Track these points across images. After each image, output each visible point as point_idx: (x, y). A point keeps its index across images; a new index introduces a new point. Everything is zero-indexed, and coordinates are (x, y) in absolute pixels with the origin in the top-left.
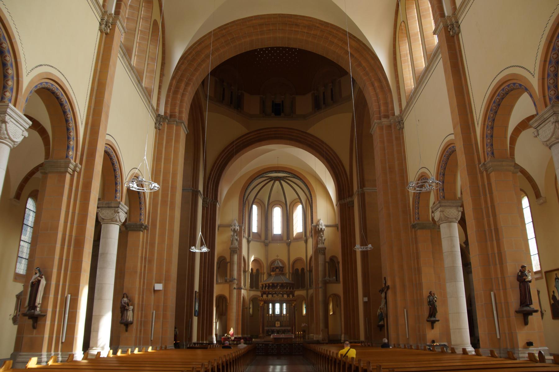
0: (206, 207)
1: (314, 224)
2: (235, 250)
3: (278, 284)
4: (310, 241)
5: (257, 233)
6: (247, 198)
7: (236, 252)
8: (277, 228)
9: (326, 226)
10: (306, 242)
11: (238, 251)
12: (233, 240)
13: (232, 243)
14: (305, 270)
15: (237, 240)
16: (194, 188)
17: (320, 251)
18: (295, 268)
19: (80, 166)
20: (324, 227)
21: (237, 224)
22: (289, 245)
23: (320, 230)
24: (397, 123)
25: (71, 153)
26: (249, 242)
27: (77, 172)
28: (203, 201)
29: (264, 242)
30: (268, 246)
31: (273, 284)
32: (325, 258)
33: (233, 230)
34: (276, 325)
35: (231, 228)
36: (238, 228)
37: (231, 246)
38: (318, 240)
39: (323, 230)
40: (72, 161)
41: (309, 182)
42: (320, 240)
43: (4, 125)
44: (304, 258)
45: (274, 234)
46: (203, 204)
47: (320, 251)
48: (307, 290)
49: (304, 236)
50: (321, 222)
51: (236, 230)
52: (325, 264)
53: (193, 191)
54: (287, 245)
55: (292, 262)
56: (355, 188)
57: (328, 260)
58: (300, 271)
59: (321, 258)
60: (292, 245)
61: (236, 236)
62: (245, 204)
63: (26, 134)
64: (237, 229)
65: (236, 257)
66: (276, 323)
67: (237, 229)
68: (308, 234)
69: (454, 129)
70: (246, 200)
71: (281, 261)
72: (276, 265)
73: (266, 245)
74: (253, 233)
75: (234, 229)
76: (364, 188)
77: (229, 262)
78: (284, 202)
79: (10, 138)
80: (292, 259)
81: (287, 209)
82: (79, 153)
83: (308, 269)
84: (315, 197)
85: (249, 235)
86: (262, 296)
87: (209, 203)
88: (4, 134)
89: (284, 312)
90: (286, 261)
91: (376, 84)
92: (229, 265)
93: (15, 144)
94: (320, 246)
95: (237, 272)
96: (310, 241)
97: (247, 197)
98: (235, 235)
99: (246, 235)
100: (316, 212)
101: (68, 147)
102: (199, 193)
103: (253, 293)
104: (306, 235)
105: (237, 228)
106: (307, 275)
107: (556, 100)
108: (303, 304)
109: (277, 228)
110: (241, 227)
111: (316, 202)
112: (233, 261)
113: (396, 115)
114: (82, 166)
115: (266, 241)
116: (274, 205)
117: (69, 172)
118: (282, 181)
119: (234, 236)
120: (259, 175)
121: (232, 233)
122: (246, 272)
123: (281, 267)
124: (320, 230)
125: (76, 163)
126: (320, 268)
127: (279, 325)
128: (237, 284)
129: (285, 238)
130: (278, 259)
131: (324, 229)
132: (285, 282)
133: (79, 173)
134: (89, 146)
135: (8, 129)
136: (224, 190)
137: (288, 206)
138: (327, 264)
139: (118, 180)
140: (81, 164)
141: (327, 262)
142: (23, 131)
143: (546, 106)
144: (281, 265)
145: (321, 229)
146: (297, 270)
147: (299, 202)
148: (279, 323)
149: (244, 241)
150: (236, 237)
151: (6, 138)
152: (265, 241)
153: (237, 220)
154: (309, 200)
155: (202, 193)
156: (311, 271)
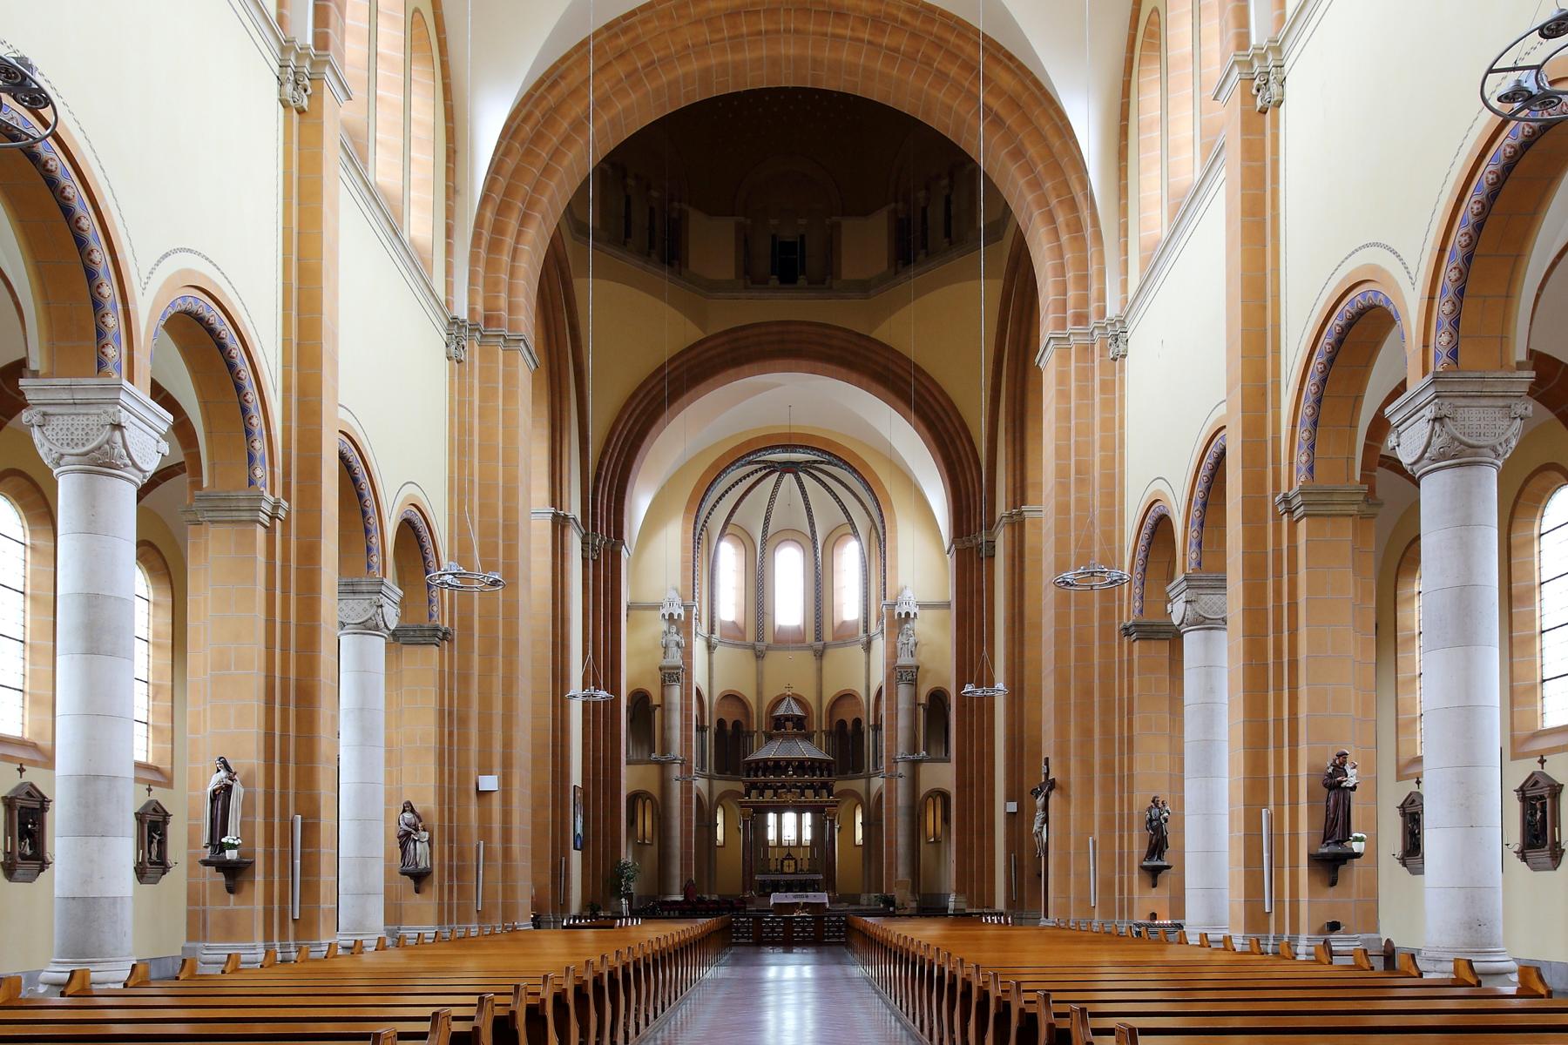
0: (594, 560)
1: (888, 601)
2: (675, 672)
3: (789, 762)
4: (880, 647)
5: (734, 622)
6: (704, 525)
7: (678, 679)
8: (789, 611)
9: (922, 606)
10: (868, 647)
11: (682, 676)
12: (666, 647)
13: (665, 653)
14: (864, 725)
15: (678, 644)
16: (559, 508)
18: (837, 718)
19: (285, 504)
20: (913, 610)
21: (678, 601)
22: (820, 655)
23: (903, 616)
24: (1110, 341)
25: (259, 472)
26: (710, 647)
27: (281, 520)
28: (582, 543)
29: (754, 649)
31: (777, 762)
32: (916, 696)
33: (667, 617)
35: (663, 611)
37: (664, 663)
38: (899, 645)
39: (912, 616)
40: (267, 494)
43: (117, 434)
46: (582, 550)
48: (868, 778)
50: (908, 594)
51: (676, 617)
53: (555, 516)
55: (828, 701)
56: (1001, 509)
57: (923, 699)
58: (849, 726)
59: (903, 691)
60: (830, 652)
62: (698, 543)
63: (165, 448)
64: (679, 615)
65: (676, 693)
67: (679, 615)
68: (873, 629)
69: (1228, 394)
70: (702, 530)
71: (799, 700)
72: (781, 711)
73: (759, 656)
74: (724, 625)
75: (671, 615)
76: (1024, 508)
77: (659, 706)
78: (809, 534)
79: (135, 465)
80: (829, 694)
81: (815, 555)
82: (279, 470)
84: (894, 522)
85: (712, 631)
86: (748, 794)
87: (600, 550)
88: (121, 457)
89: (807, 835)
90: (810, 696)
91: (1061, 218)
92: (658, 712)
93: (144, 477)
94: (904, 660)
95: (681, 731)
96: (880, 647)
97: (706, 522)
98: (675, 630)
99: (704, 630)
100: (895, 567)
101: (251, 458)
102: (572, 520)
103: (721, 786)
104: (866, 630)
105: (679, 611)
106: (869, 738)
107: (1448, 360)
108: (857, 812)
109: (789, 611)
110: (688, 609)
111: (895, 538)
112: (670, 703)
113: (1108, 316)
114: (290, 505)
115: (760, 646)
116: (779, 544)
117: (262, 521)
119: (669, 632)
120: (738, 460)
121: (664, 626)
123: (800, 718)
124: (903, 616)
125: (276, 497)
126: (903, 721)
129: (810, 638)
130: (789, 696)
131: (915, 614)
133: (286, 523)
134: (299, 449)
135: (128, 444)
136: (640, 503)
138: (921, 710)
139: (371, 521)
140: (287, 497)
141: (919, 705)
142: (158, 442)
143: (1425, 373)
144: (797, 711)
145: (908, 614)
146: (842, 723)
147: (851, 534)
149: (699, 647)
150: (677, 638)
151: (126, 466)
152: (756, 643)
153: (677, 590)
154: (876, 529)
155: (579, 520)
156: (877, 728)
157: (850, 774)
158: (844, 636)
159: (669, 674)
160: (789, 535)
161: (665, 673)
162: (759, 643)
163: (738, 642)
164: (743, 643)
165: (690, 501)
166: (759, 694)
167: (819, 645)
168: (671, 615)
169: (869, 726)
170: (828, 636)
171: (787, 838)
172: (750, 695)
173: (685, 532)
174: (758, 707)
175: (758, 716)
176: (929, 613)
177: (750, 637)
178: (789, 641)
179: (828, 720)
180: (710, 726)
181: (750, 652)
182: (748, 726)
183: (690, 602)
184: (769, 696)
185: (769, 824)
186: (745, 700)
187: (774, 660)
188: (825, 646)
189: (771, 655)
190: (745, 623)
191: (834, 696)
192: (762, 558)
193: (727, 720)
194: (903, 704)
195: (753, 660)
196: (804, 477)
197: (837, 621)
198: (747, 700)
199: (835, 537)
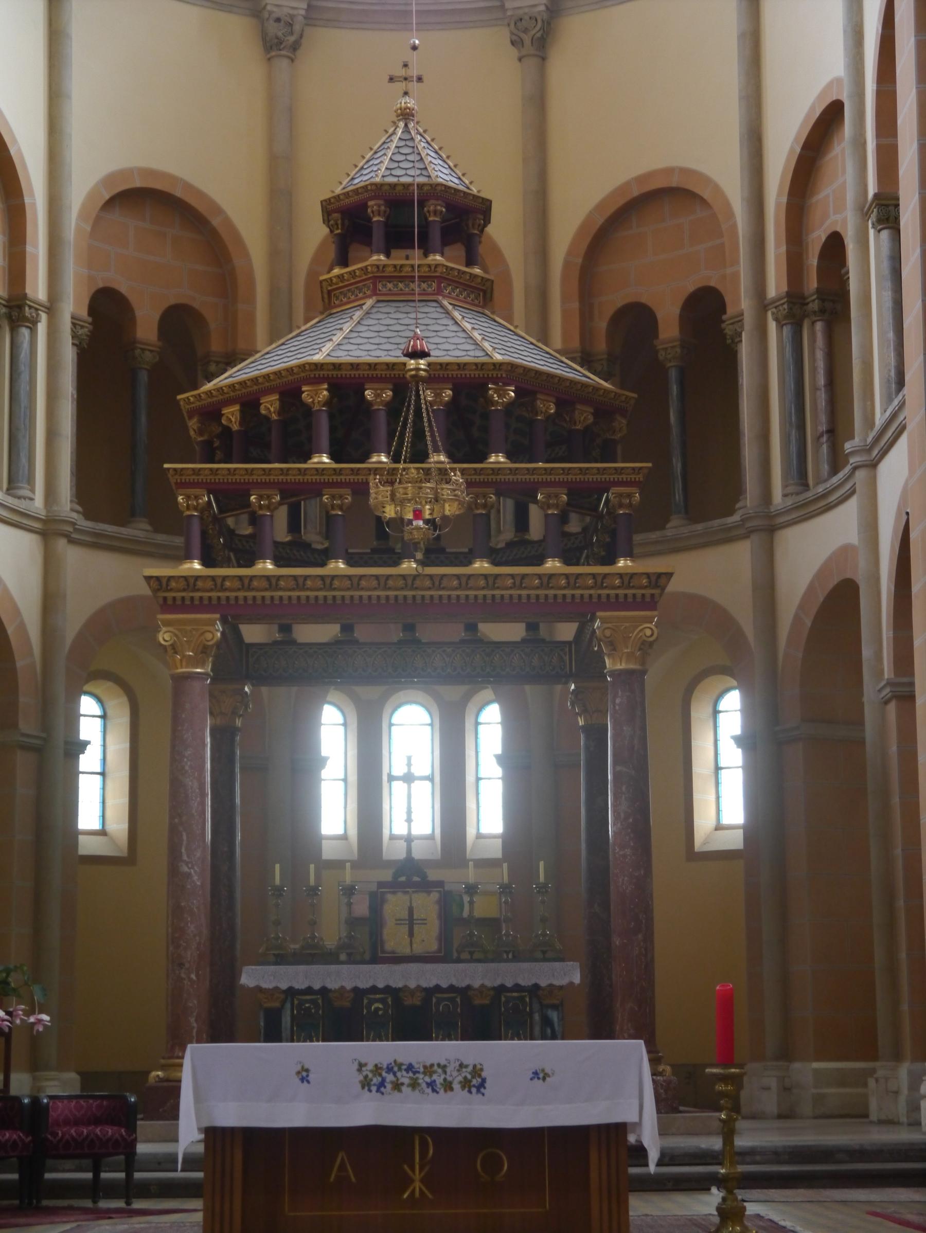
30: (295, 47)
83: (775, 285)
108: (694, 714)
122: (33, 324)
132: (498, 357)
157: (676, 526)
169: (762, 305)
171: (400, 829)
174: (274, 254)
175: (273, 291)
179: (575, 305)
180: (51, 308)
185: (324, 752)
186: (216, 222)
191: (600, 207)
193: (133, 299)
198: (228, 222)
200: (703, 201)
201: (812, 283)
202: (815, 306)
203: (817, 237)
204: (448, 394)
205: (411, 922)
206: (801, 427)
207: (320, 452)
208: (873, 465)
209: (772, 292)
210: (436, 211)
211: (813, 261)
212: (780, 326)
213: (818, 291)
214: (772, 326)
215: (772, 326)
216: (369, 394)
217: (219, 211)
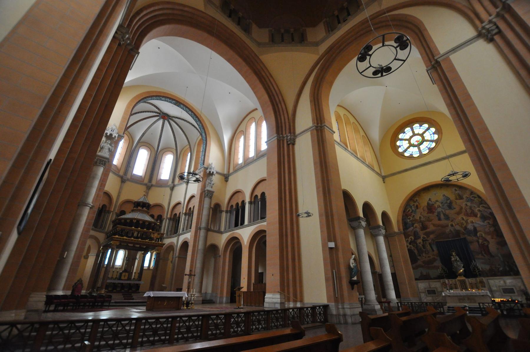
2: (105, 160)
7: (105, 164)
9: (217, 173)
15: (109, 149)
17: (208, 194)
23: (211, 173)
34: (123, 278)
36: (117, 136)
38: (207, 183)
41: (207, 127)
42: (209, 183)
44: (166, 205)
45: (134, 174)
47: (208, 194)
48: (179, 235)
49: (170, 183)
51: (113, 136)
52: (210, 209)
54: (147, 188)
57: (212, 206)
60: (153, 189)
61: (110, 145)
64: (115, 136)
66: (124, 274)
75: (111, 135)
83: (169, 216)
84: (210, 142)
94: (208, 188)
98: (109, 143)
100: (209, 156)
115: (125, 178)
118: (170, 120)
127: (126, 278)
128: (91, 208)
129: (146, 181)
137: (158, 153)
141: (211, 208)
148: (127, 274)
150: (109, 145)
158: (162, 184)
159: (101, 160)
160: (147, 145)
161: (99, 159)
162: (125, 176)
163: (116, 173)
164: (117, 173)
165: (135, 98)
166: (119, 196)
167: (150, 184)
168: (111, 135)
169: (167, 218)
170: (154, 182)
172: (114, 195)
173: (128, 107)
176: (216, 175)
177: (121, 173)
178: (137, 180)
181: (119, 179)
182: (110, 208)
183: (122, 134)
184: (123, 198)
187: (128, 185)
188: (152, 186)
189: (128, 184)
190: (121, 167)
192: (136, 147)
194: (206, 205)
195: (120, 183)
196: (166, 122)
197: (158, 178)
199: (167, 150)
200: (163, 207)
201: (172, 217)
202: (172, 219)
203: (174, 213)
204: (148, 223)
205: (125, 276)
206: (168, 230)
207: (133, 226)
208: (179, 236)
209: (168, 217)
210: (147, 205)
211: (173, 215)
212: (168, 220)
213: (173, 218)
214: (167, 220)
215: (167, 220)
216: (140, 222)
217: (112, 196)
